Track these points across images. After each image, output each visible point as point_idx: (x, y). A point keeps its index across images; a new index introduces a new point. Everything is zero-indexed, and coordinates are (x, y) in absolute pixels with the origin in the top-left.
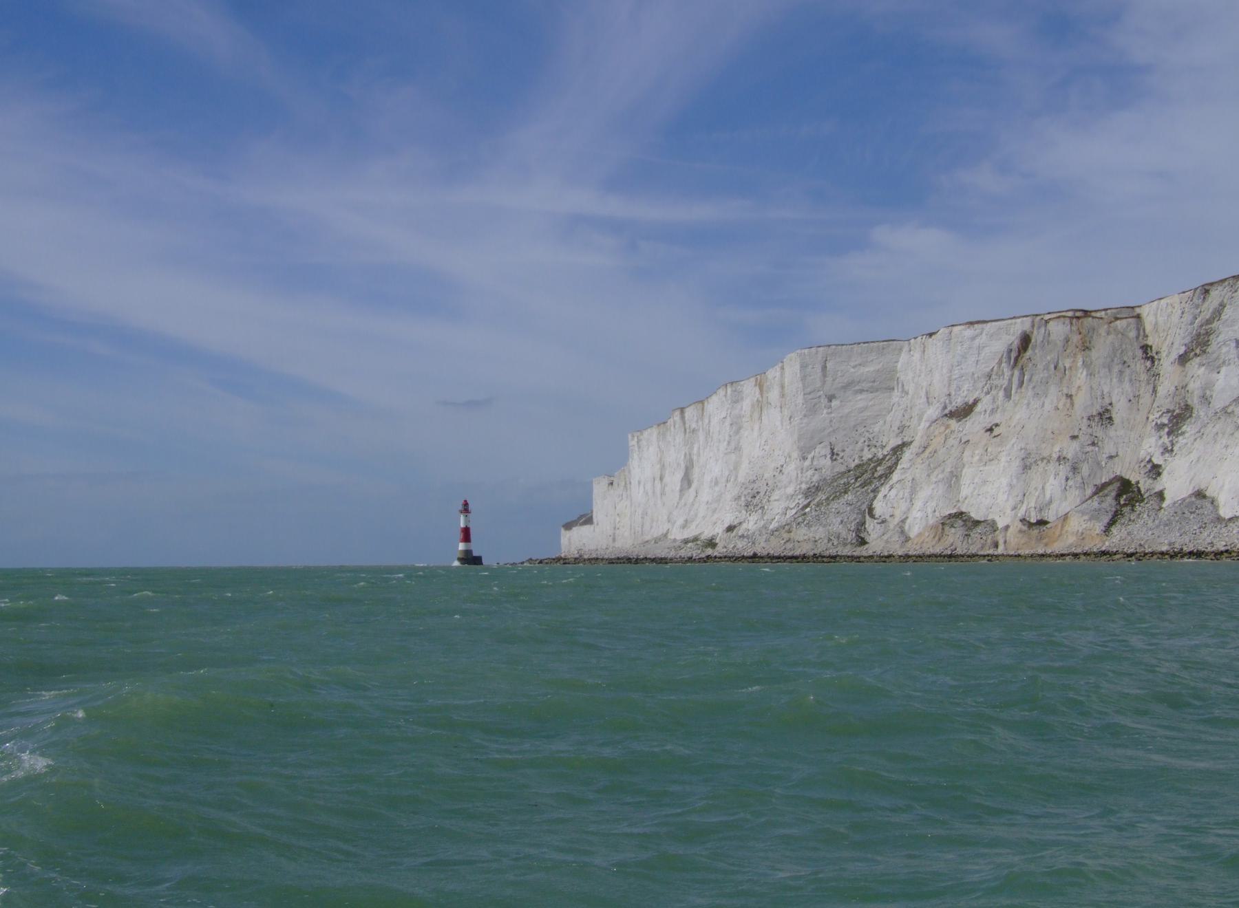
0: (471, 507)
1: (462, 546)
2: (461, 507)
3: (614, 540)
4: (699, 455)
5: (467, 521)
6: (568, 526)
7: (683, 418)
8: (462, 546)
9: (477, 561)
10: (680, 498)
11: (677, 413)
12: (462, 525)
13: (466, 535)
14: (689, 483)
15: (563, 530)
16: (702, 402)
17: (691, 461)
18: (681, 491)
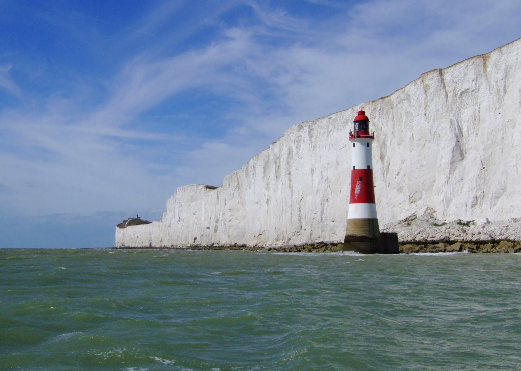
0: (372, 128)
1: (357, 211)
2: (351, 127)
3: (216, 231)
4: (476, 119)
5: (368, 156)
6: (121, 226)
7: (443, 80)
8: (357, 211)
9: (388, 243)
10: (452, 171)
11: (435, 75)
12: (360, 166)
13: (364, 186)
14: (462, 156)
15: (117, 229)
16: (484, 57)
17: (460, 128)
18: (452, 163)
